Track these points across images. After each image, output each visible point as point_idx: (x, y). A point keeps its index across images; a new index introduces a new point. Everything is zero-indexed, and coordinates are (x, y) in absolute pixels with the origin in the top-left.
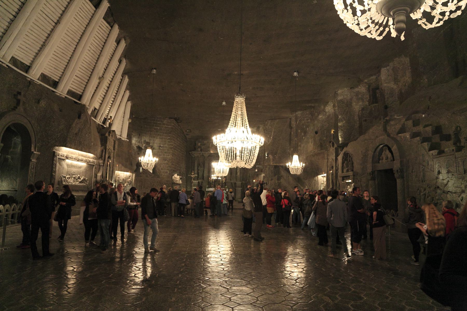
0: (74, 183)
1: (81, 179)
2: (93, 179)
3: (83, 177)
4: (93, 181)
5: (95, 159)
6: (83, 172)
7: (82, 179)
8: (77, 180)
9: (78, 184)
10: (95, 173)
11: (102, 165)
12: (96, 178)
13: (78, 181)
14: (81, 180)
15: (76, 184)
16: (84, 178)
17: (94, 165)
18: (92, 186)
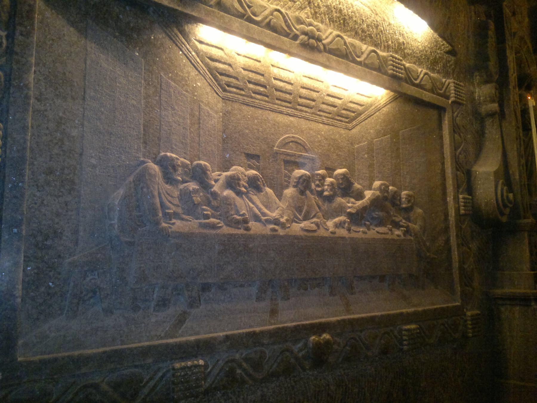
0: (297, 228)
1: (359, 196)
2: (450, 199)
3: (377, 184)
4: (452, 212)
5: (447, 75)
6: (370, 150)
7: (368, 194)
8: (330, 199)
9: (343, 232)
10: (456, 159)
11: (492, 115)
12: (470, 190)
13: (340, 210)
14: (359, 203)
15: (322, 232)
16: (384, 189)
17: (440, 110)
18: (448, 241)
